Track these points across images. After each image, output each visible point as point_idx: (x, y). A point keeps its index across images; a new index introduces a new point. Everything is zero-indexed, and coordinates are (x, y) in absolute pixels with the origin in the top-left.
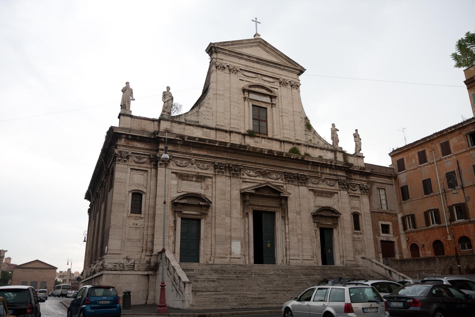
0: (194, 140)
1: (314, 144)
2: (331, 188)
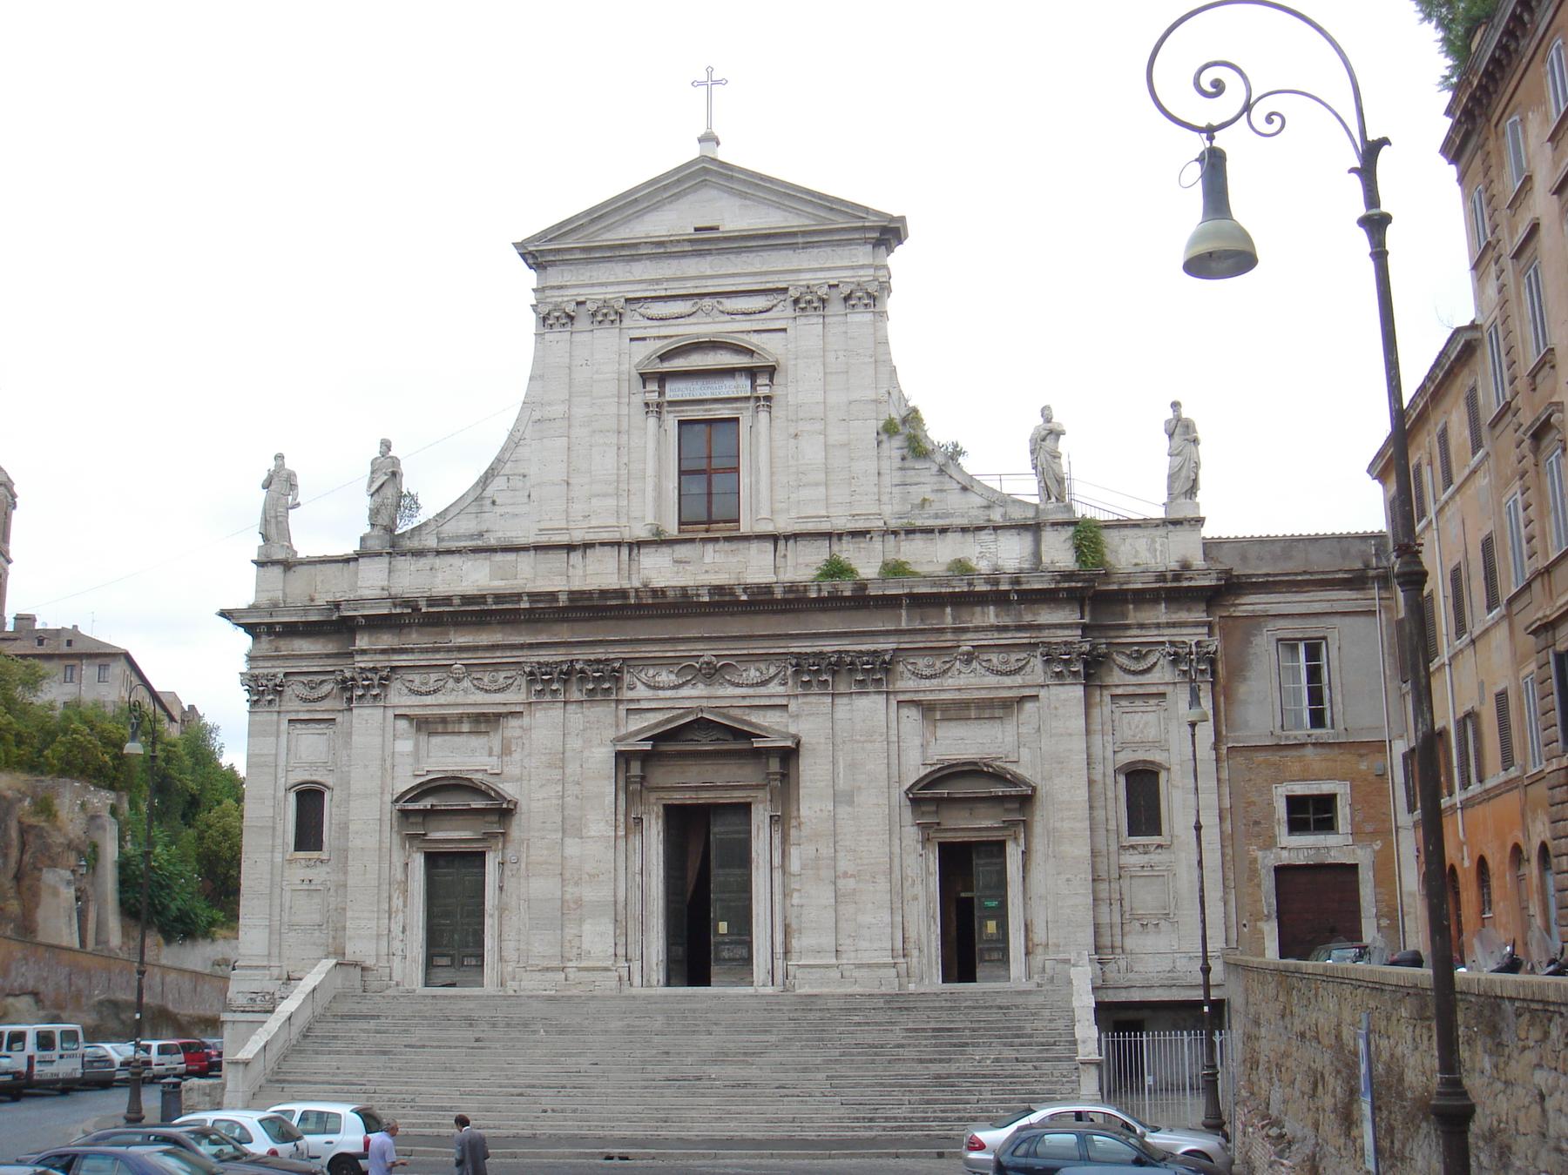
0: (451, 606)
1: (937, 516)
2: (1007, 681)
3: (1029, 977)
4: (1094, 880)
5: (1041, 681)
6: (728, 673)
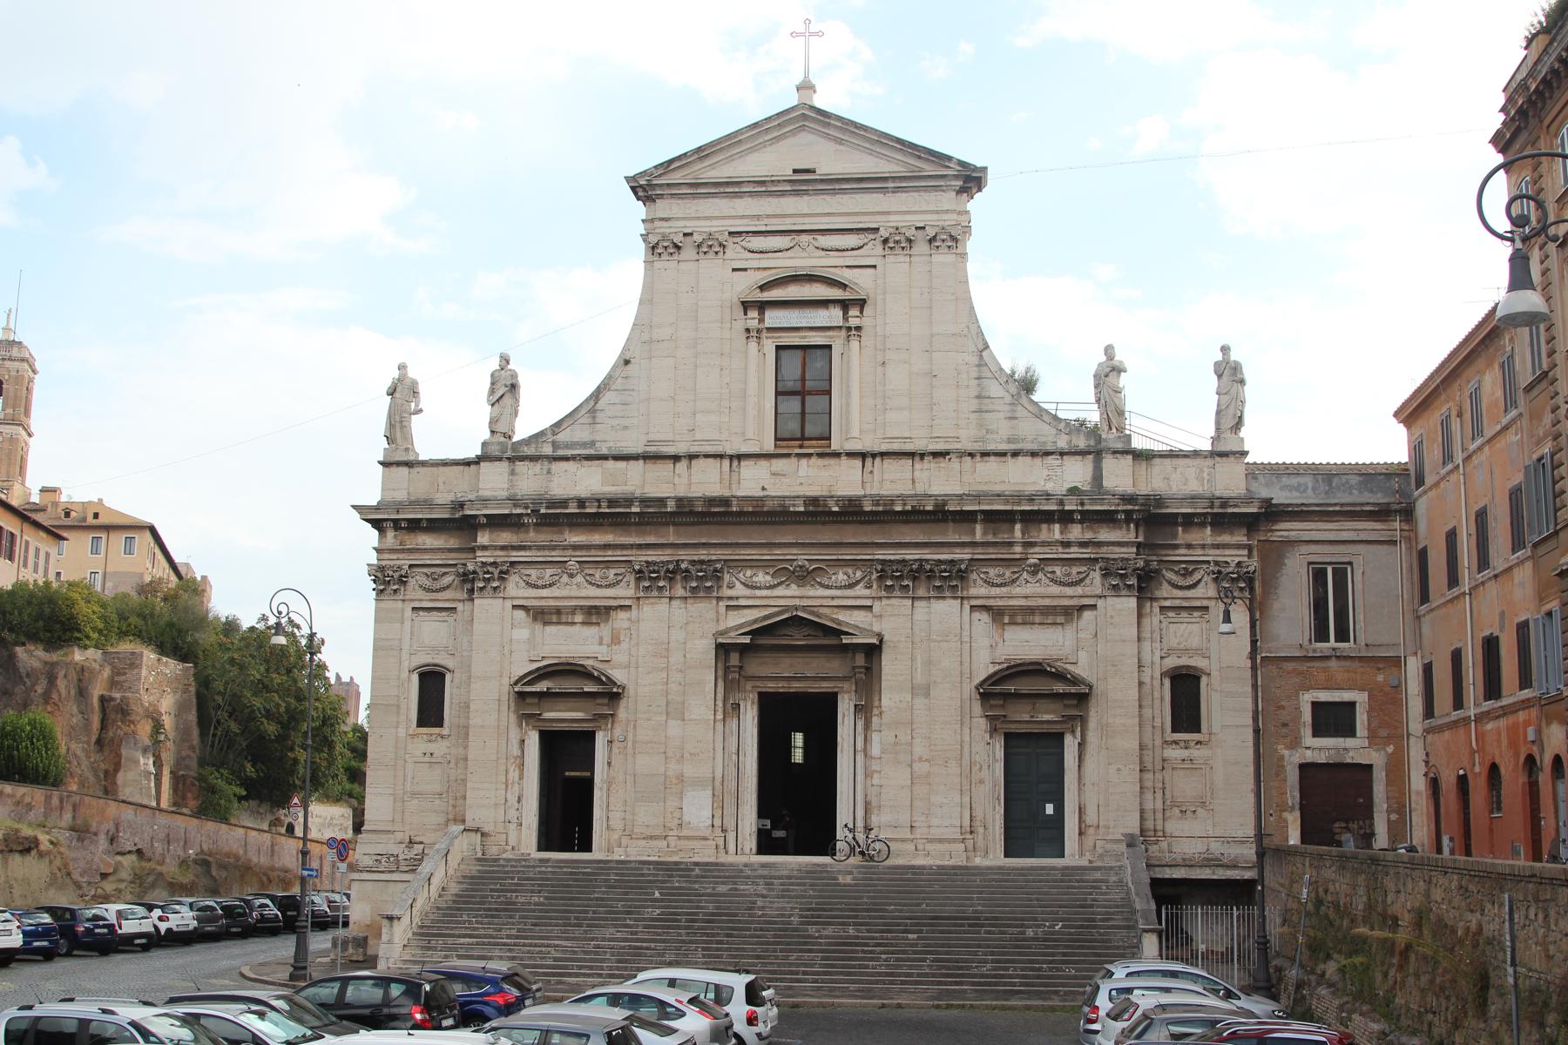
2: (1069, 591)
3: (1081, 854)
4: (1141, 771)
5: (1099, 592)
6: (818, 576)
